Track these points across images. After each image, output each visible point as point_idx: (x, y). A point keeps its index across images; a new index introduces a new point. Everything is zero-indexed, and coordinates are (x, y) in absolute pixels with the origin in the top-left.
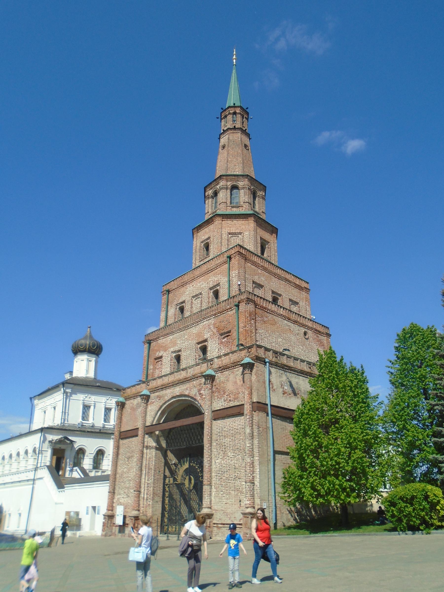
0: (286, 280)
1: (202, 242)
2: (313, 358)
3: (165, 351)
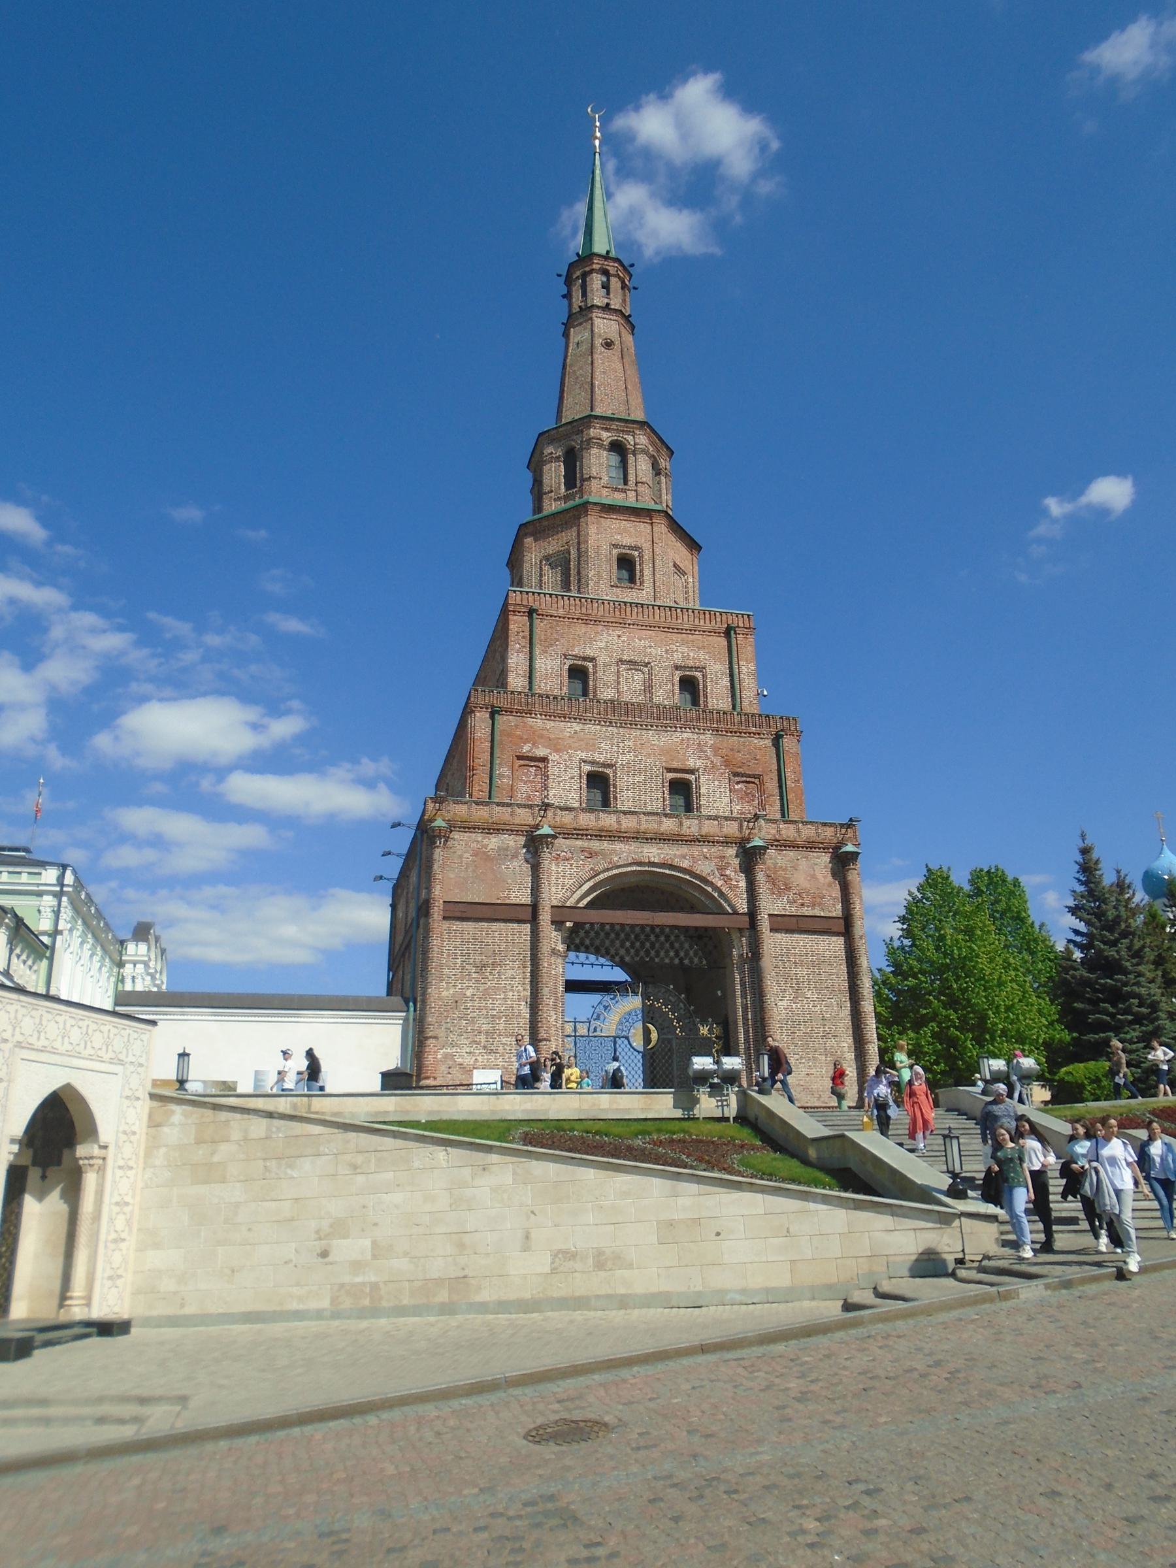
1: (616, 546)
3: (558, 751)
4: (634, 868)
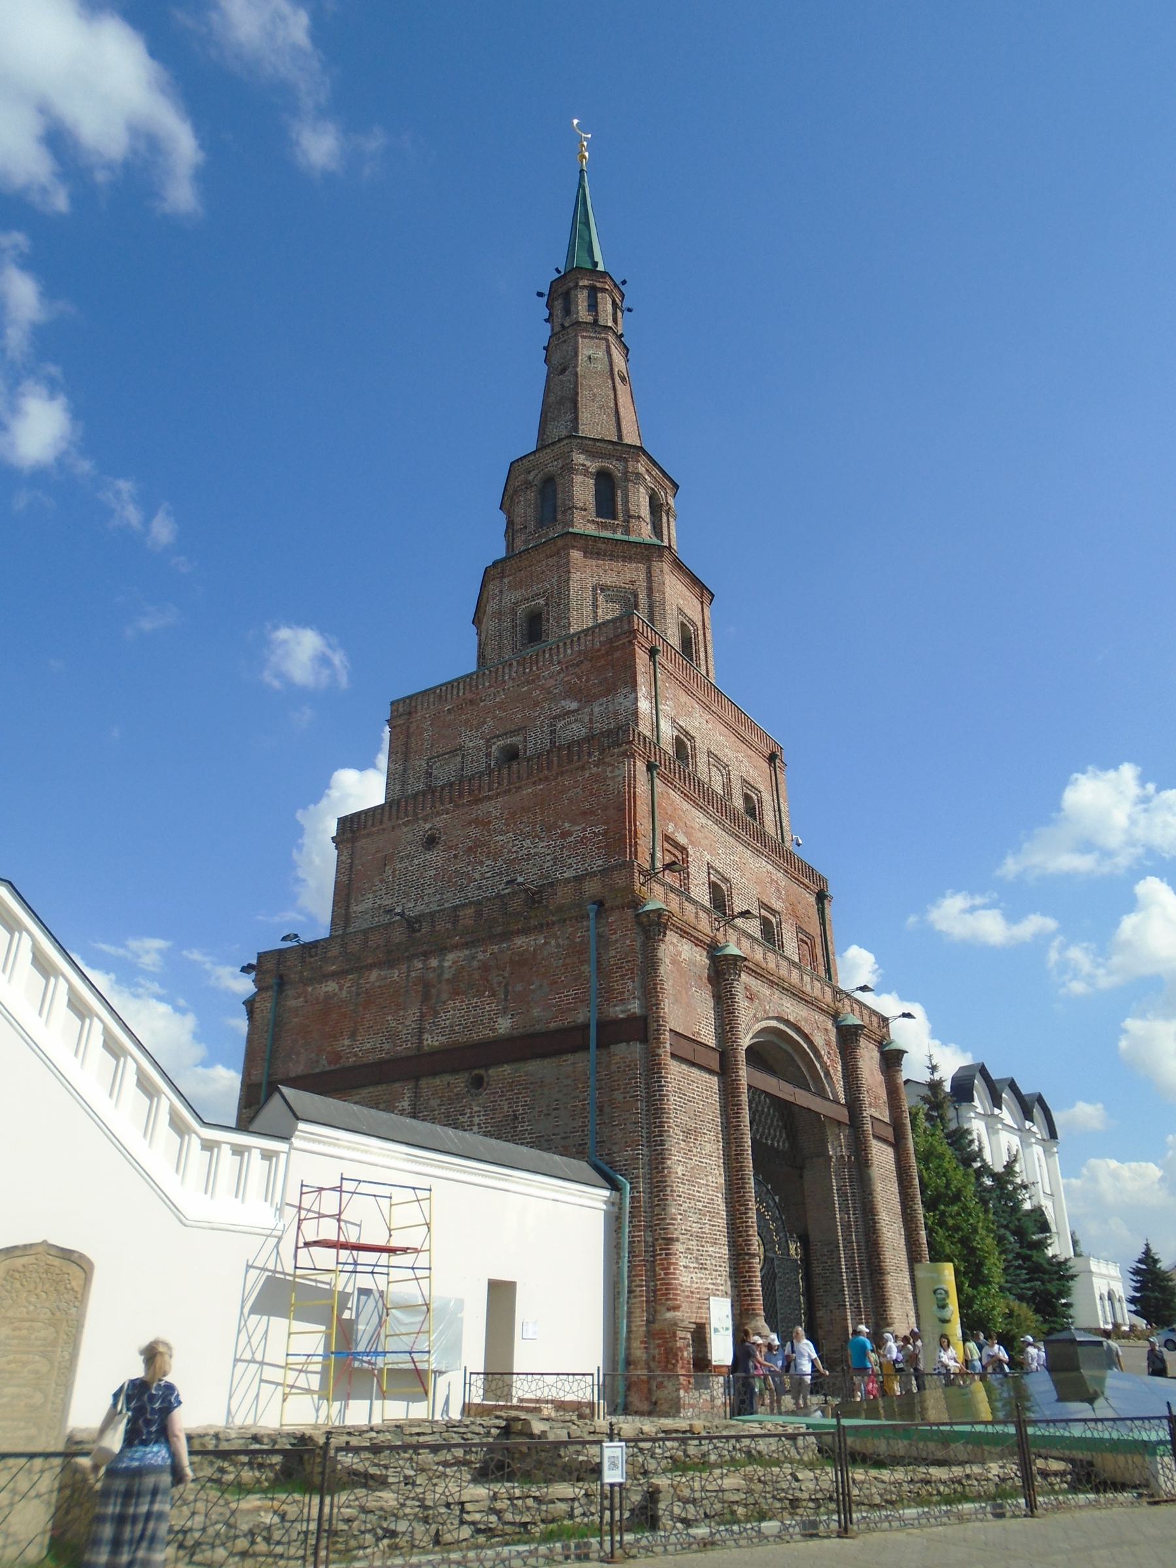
3: (692, 843)
4: (774, 1023)
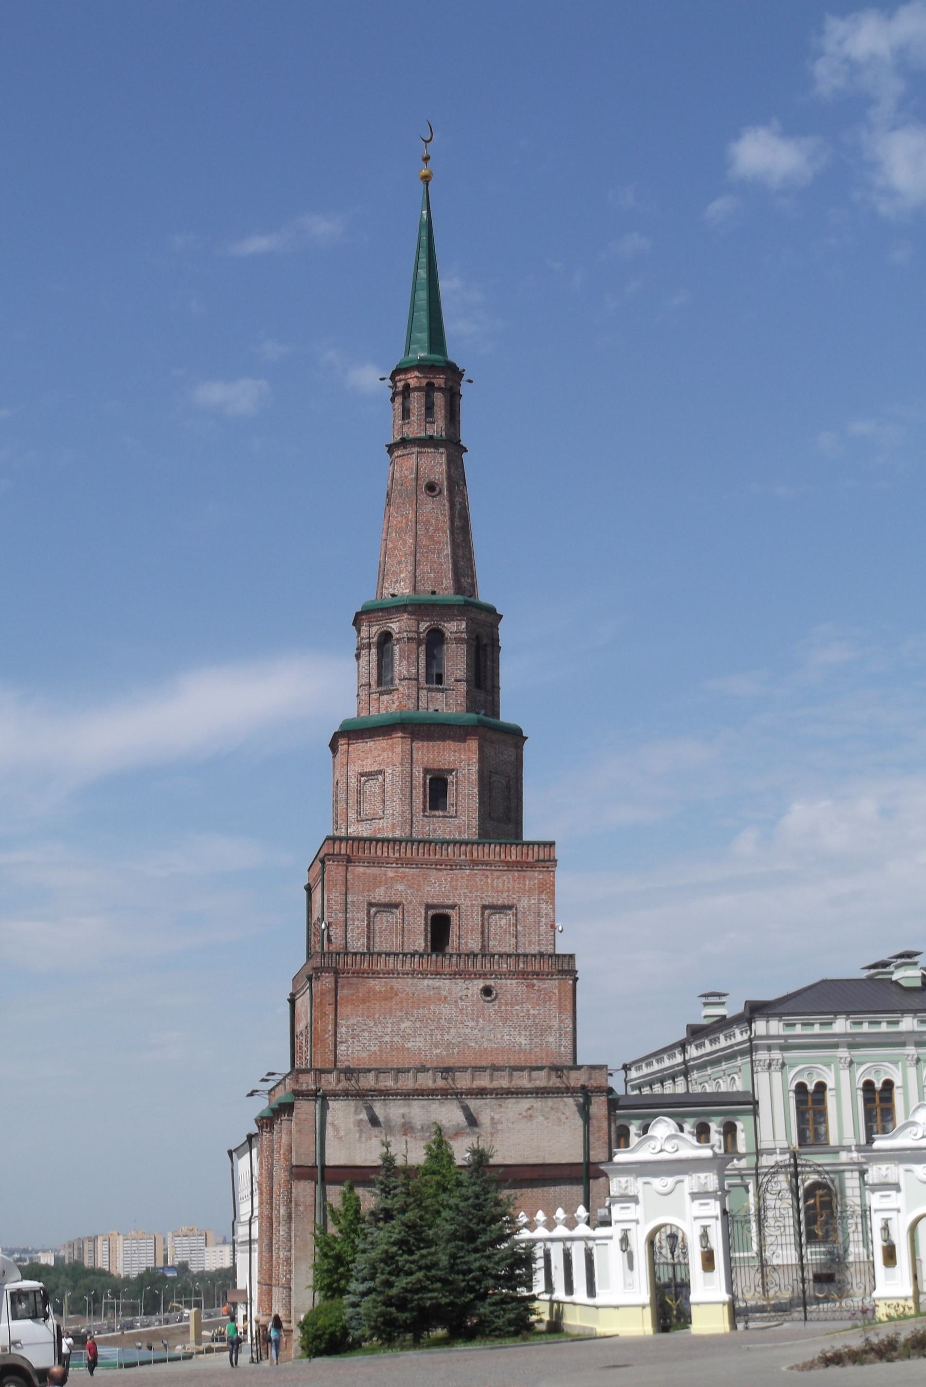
0: (475, 863)
2: (506, 1038)
